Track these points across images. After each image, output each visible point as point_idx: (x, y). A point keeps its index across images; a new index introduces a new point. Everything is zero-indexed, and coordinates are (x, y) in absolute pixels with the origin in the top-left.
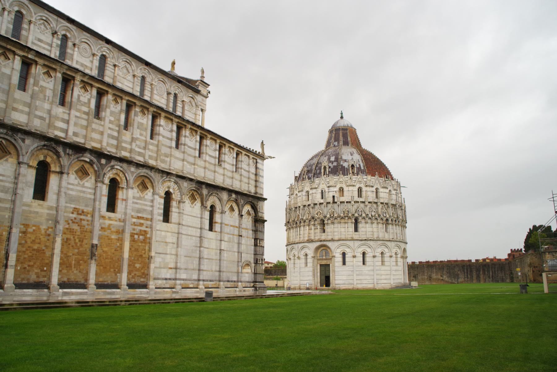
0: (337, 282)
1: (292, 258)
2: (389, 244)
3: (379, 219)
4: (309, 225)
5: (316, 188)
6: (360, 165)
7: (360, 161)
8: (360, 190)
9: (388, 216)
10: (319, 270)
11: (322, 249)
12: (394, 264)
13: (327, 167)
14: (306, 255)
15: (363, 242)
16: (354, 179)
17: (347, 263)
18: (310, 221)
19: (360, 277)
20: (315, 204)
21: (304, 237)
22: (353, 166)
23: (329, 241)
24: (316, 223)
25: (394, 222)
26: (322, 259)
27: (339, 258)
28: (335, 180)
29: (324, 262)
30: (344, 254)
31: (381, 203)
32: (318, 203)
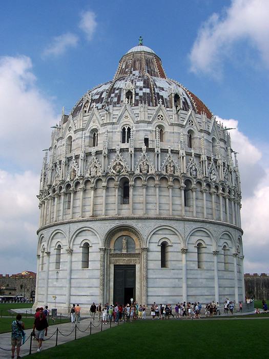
1: (53, 251)
4: (95, 189)
6: (185, 98)
7: (185, 94)
10: (112, 276)
11: (120, 234)
14: (86, 246)
15: (199, 225)
17: (169, 264)
18: (99, 180)
20: (111, 151)
21: (83, 211)
24: (112, 185)
26: (121, 255)
27: (156, 255)
29: (122, 261)
30: (164, 246)
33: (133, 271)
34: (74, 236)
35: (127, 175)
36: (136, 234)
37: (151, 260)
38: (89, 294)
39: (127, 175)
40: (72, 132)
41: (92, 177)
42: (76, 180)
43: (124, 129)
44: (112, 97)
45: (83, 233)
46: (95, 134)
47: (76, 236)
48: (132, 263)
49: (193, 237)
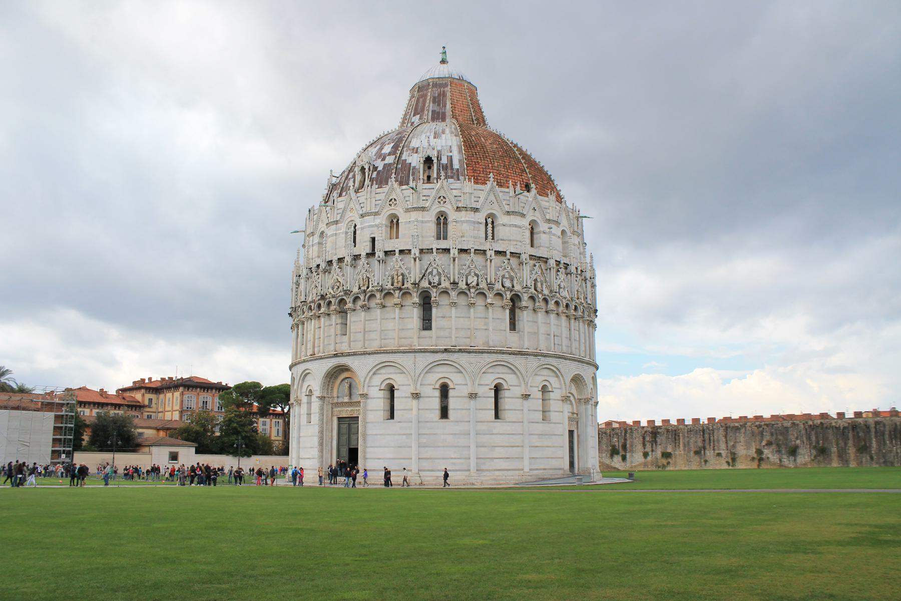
2: (518, 361)
3: (490, 295)
5: (336, 222)
6: (450, 159)
8: (442, 221)
9: (517, 288)
12: (539, 415)
13: (367, 167)
16: (426, 192)
19: (428, 453)
20: (330, 263)
22: (428, 161)
23: (355, 354)
25: (561, 309)
26: (343, 404)
27: (377, 402)
28: (378, 197)
29: (346, 412)
31: (498, 253)
32: (335, 259)
45: (308, 377)
49: (430, 375)
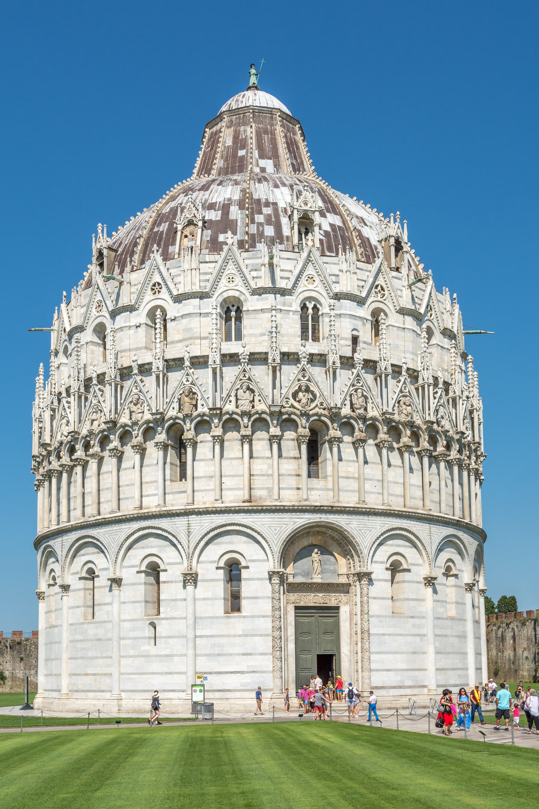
0: (377, 679)
10: (291, 631)
20: (289, 358)
33: (332, 620)
34: (202, 543)
35: (325, 416)
36: (340, 544)
37: (375, 598)
38: (246, 670)
39: (325, 416)
40: (164, 294)
41: (244, 414)
42: (199, 415)
43: (304, 307)
44: (260, 224)
46: (228, 311)
47: (207, 544)
48: (333, 603)
